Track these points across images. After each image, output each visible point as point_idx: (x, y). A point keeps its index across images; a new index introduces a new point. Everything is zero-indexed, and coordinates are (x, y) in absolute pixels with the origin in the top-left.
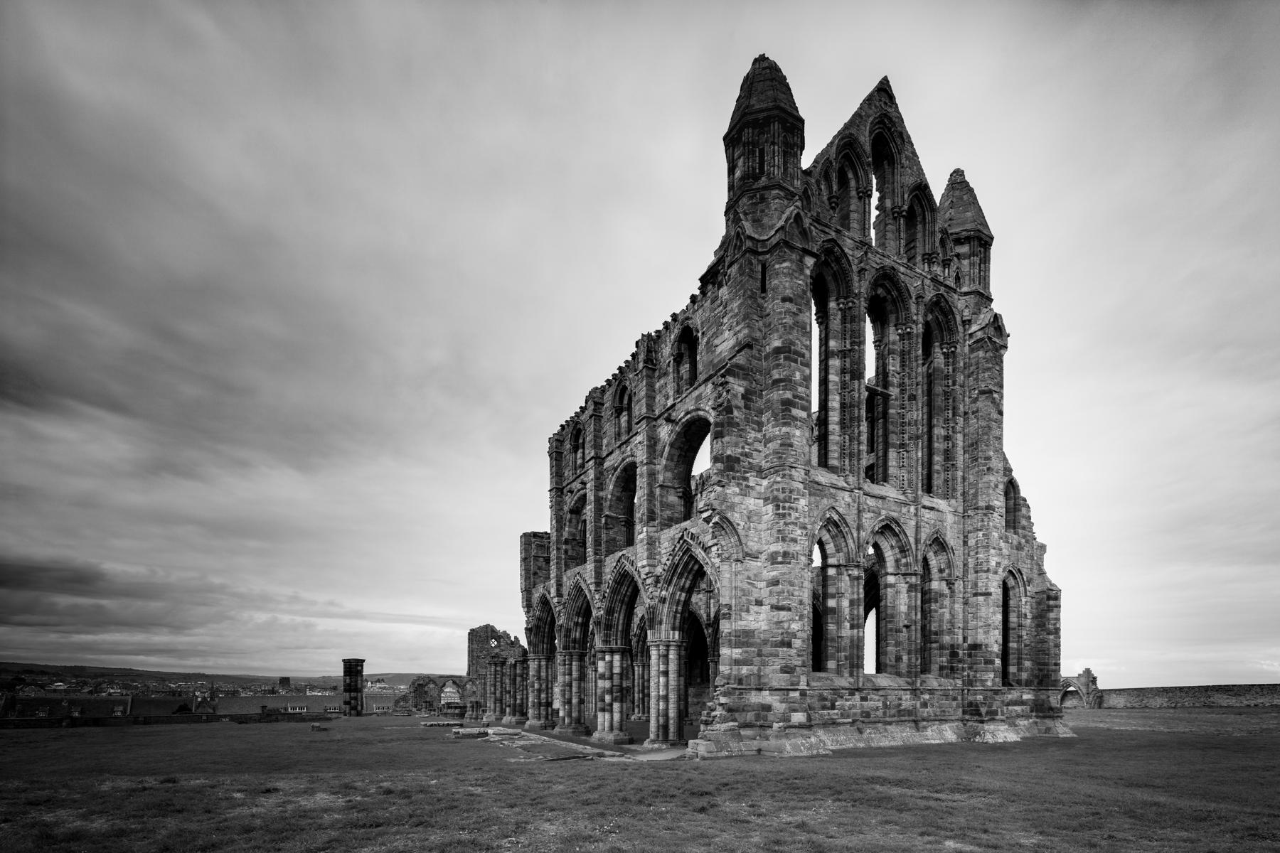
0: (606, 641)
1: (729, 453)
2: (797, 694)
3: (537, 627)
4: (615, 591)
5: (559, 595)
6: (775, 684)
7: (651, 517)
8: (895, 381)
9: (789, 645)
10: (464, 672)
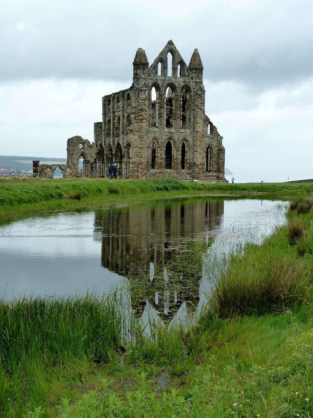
0: (115, 160)
1: (131, 129)
2: (144, 173)
3: (99, 153)
4: (117, 147)
5: (105, 145)
6: (140, 171)
7: (123, 132)
8: (174, 105)
9: (142, 164)
10: (65, 163)
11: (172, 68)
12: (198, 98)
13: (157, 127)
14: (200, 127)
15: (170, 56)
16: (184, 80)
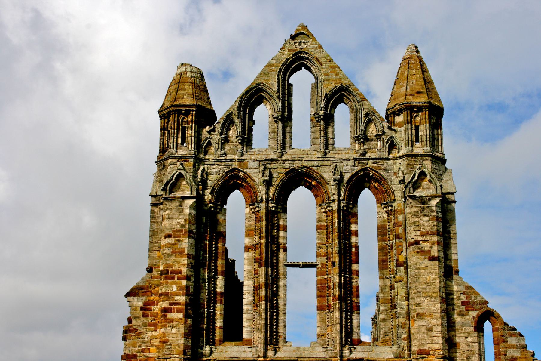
11: (312, 120)
12: (416, 214)
13: (249, 343)
14: (430, 330)
15: (301, 81)
16: (358, 156)
